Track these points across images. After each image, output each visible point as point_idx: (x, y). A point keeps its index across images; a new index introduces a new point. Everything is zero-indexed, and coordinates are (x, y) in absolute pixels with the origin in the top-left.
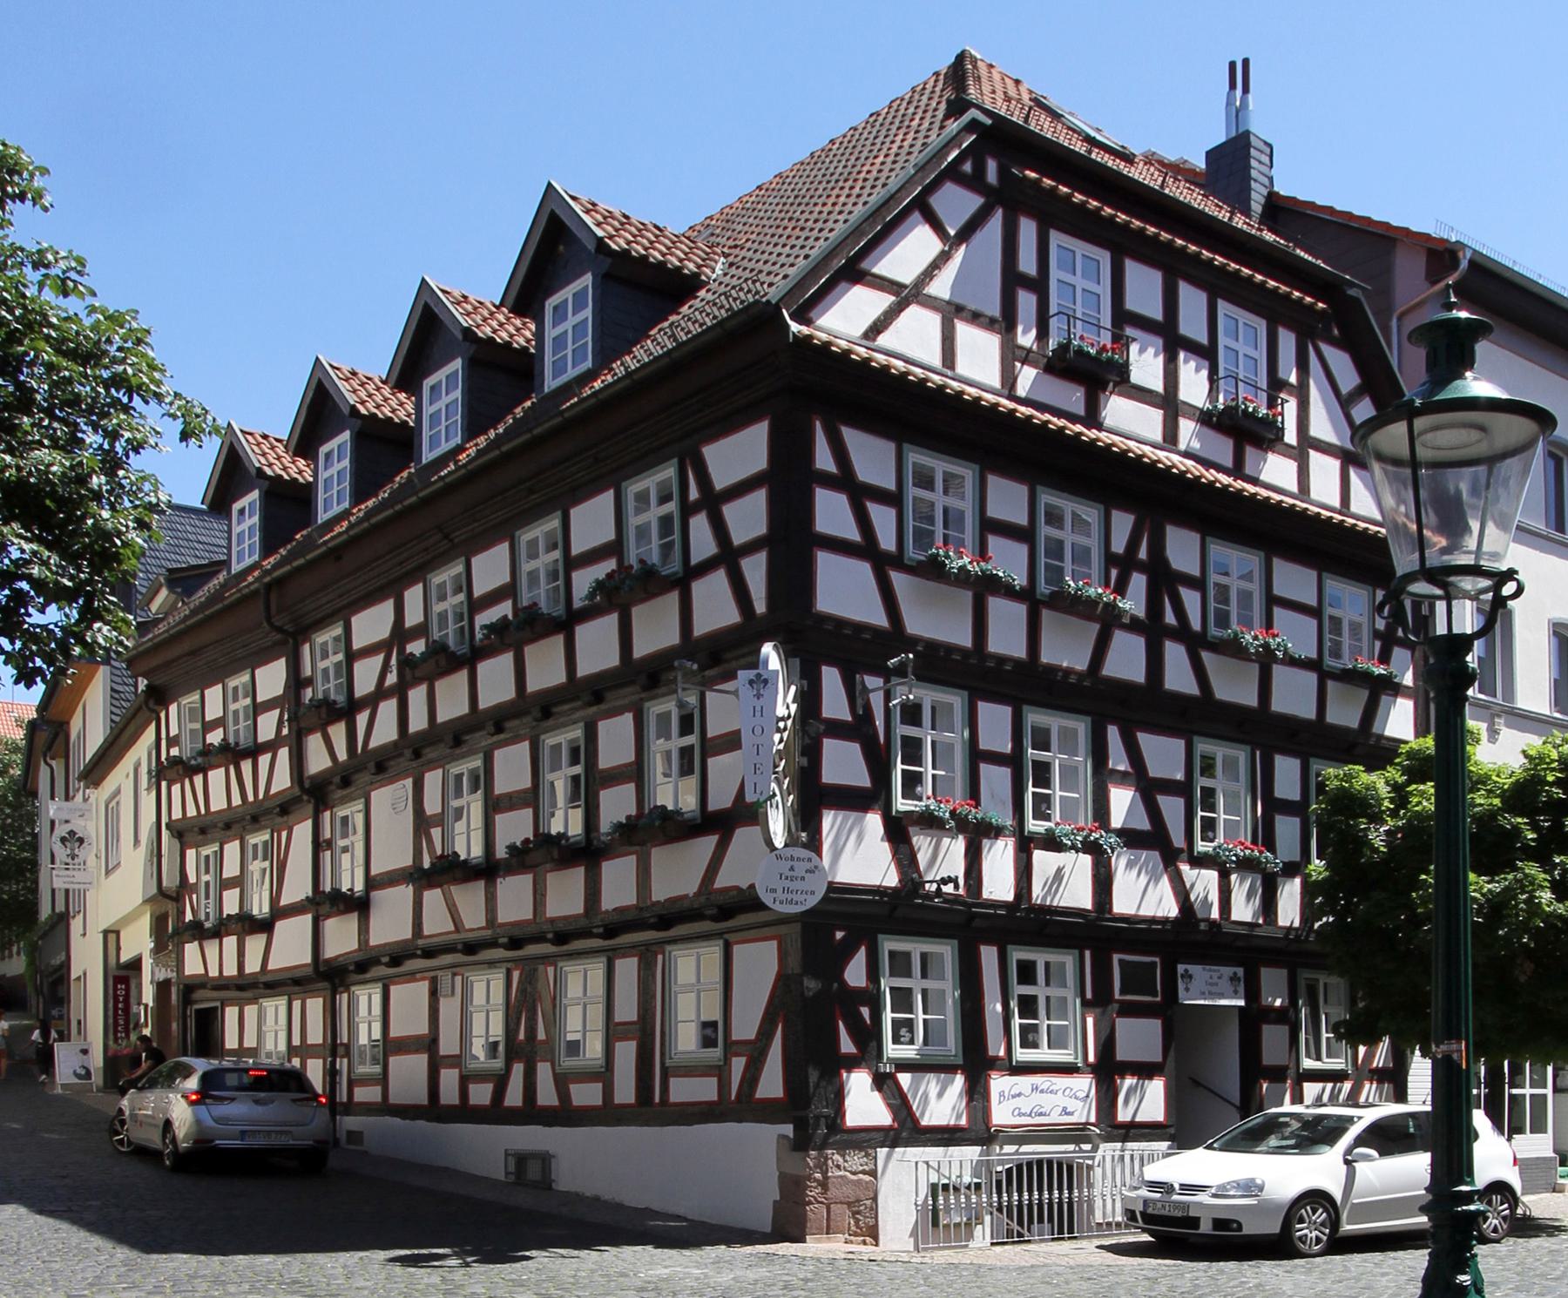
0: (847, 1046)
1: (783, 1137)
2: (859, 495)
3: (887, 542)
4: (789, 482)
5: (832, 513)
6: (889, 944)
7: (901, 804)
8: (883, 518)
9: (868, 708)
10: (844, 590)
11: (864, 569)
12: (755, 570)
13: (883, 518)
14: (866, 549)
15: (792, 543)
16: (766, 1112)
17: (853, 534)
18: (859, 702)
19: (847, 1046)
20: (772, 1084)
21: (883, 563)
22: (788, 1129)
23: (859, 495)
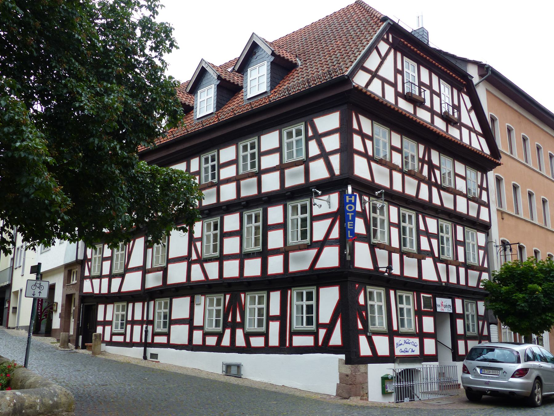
0: (360, 326)
1: (340, 360)
2: (364, 137)
3: (370, 153)
4: (346, 131)
5: (357, 143)
6: (369, 289)
7: (373, 241)
8: (369, 143)
9: (365, 207)
10: (361, 168)
11: (364, 161)
12: (335, 160)
13: (369, 143)
14: (364, 155)
15: (347, 152)
16: (335, 350)
17: (362, 149)
18: (363, 205)
19: (360, 326)
20: (336, 339)
21: (370, 159)
22: (343, 357)
23: (364, 137)
